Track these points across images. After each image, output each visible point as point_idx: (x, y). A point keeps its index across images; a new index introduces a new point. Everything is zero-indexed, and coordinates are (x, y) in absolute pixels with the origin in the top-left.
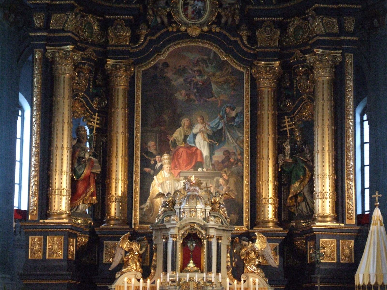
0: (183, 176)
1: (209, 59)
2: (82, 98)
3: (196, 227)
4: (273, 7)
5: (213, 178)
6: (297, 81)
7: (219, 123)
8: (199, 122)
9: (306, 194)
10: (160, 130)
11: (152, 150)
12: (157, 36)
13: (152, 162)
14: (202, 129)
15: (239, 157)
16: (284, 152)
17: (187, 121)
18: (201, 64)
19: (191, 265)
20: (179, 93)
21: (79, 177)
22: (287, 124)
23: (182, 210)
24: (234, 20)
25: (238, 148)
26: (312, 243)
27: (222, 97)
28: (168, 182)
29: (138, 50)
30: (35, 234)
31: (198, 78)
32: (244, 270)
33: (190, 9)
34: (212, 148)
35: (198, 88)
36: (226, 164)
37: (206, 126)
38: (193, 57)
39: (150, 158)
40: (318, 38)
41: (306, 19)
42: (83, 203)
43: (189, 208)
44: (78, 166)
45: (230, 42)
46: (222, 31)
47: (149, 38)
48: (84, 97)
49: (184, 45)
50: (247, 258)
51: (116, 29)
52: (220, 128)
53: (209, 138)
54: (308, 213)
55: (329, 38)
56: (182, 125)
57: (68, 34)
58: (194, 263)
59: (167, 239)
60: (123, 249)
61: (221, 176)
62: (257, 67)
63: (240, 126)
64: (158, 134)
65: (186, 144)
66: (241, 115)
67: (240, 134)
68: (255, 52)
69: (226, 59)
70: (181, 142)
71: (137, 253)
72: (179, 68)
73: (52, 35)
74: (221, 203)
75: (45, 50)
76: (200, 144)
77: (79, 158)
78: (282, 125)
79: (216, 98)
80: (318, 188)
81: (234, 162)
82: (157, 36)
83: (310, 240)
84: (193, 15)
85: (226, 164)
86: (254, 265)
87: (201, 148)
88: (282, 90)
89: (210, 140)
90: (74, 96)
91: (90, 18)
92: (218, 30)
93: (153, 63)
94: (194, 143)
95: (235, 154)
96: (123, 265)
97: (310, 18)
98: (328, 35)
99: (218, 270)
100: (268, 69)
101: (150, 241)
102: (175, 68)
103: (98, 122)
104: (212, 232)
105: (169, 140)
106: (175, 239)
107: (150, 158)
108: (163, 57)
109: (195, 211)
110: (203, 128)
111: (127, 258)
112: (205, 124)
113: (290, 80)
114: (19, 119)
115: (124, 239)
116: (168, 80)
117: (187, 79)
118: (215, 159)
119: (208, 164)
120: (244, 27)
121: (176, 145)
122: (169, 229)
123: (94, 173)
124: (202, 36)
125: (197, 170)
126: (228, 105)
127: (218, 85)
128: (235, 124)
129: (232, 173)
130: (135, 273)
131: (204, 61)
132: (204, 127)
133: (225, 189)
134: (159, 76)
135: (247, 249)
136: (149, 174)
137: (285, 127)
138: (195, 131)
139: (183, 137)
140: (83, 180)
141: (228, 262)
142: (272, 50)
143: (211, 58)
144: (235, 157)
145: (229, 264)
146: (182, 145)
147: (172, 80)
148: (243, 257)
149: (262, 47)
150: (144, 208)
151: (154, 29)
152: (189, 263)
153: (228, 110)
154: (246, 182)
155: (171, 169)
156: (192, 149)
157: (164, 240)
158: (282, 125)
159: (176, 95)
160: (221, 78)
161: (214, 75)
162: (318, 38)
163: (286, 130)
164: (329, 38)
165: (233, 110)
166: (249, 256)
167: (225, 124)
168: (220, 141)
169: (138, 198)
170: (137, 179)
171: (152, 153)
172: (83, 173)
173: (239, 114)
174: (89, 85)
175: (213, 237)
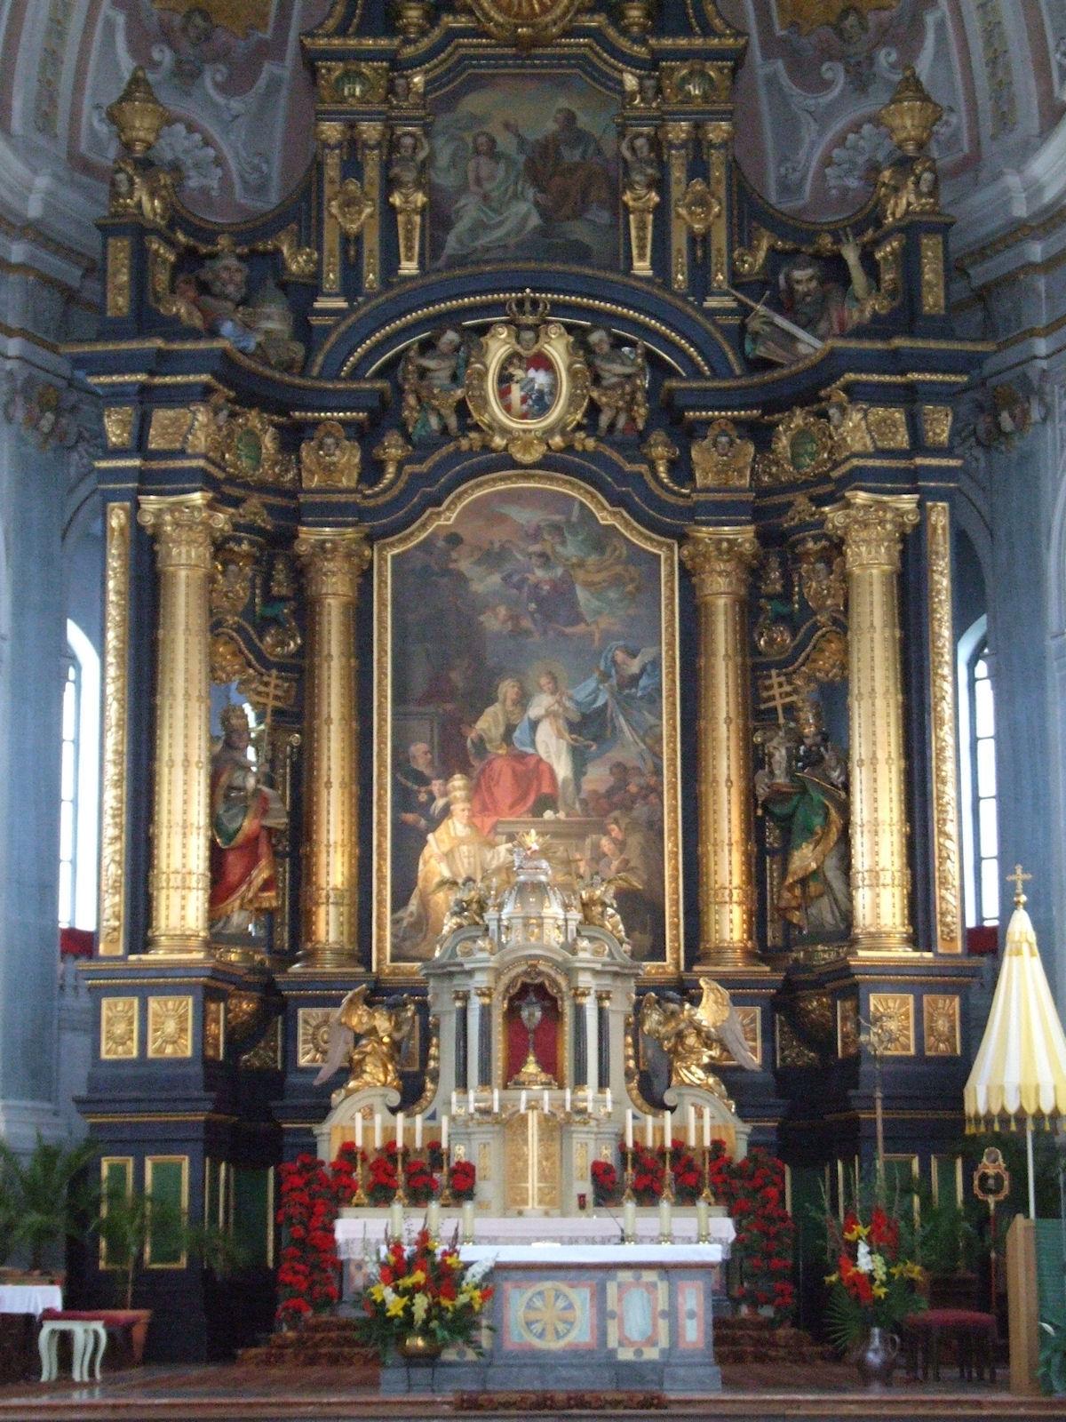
0: (503, 834)
1: (568, 521)
2: (237, 631)
3: (543, 967)
5: (582, 836)
6: (801, 577)
7: (596, 691)
10: (441, 711)
13: (423, 797)
15: (653, 780)
18: (546, 537)
19: (531, 1067)
20: (489, 613)
21: (230, 837)
22: (776, 691)
23: (505, 923)
25: (647, 756)
26: (848, 1005)
27: (604, 623)
28: (464, 848)
29: (381, 500)
30: (117, 992)
31: (540, 573)
32: (670, 1079)
33: (516, 393)
34: (580, 759)
35: (540, 601)
38: (524, 516)
40: (855, 462)
41: (823, 414)
42: (242, 907)
43: (523, 918)
45: (623, 477)
47: (408, 468)
48: (240, 629)
49: (501, 487)
50: (680, 1048)
51: (321, 447)
52: (599, 703)
53: (571, 732)
55: (886, 463)
56: (501, 697)
57: (195, 463)
58: (538, 1062)
59: (465, 997)
60: (349, 1029)
61: (607, 833)
62: (697, 541)
63: (653, 698)
67: (651, 720)
68: (689, 503)
69: (610, 521)
71: (386, 1040)
73: (154, 465)
74: (608, 901)
75: (137, 506)
77: (231, 788)
78: (765, 694)
79: (588, 625)
80: (861, 860)
81: (638, 793)
83: (845, 999)
84: (525, 407)
85: (615, 799)
86: (698, 1066)
88: (763, 600)
89: (574, 736)
90: (215, 627)
91: (254, 419)
92: (591, 443)
94: (533, 743)
95: (642, 775)
96: (349, 1070)
97: (833, 412)
99: (603, 1082)
101: (423, 1008)
103: (279, 693)
104: (585, 980)
106: (487, 1000)
107: (416, 787)
108: (447, 518)
109: (540, 926)
110: (556, 707)
111: (360, 1053)
112: (561, 695)
114: (70, 689)
115: (351, 1001)
116: (461, 578)
117: (510, 576)
119: (570, 801)
120: (658, 436)
123: (270, 830)
124: (548, 464)
126: (621, 643)
128: (639, 694)
131: (557, 529)
132: (559, 702)
133: (615, 864)
134: (436, 568)
135: (678, 1025)
137: (772, 698)
138: (534, 711)
139: (502, 730)
140: (240, 847)
141: (627, 1058)
142: (736, 497)
144: (642, 781)
145: (632, 1063)
146: (500, 752)
148: (667, 1045)
149: (707, 490)
152: (526, 1063)
153: (620, 656)
154: (672, 846)
155: (474, 816)
157: (459, 1004)
158: (765, 694)
159: (482, 618)
161: (581, 565)
162: (855, 462)
163: (775, 709)
164: (886, 463)
165: (635, 656)
166: (683, 1044)
167: (612, 694)
170: (383, 842)
172: (238, 830)
173: (649, 668)
174: (254, 594)
175: (589, 994)
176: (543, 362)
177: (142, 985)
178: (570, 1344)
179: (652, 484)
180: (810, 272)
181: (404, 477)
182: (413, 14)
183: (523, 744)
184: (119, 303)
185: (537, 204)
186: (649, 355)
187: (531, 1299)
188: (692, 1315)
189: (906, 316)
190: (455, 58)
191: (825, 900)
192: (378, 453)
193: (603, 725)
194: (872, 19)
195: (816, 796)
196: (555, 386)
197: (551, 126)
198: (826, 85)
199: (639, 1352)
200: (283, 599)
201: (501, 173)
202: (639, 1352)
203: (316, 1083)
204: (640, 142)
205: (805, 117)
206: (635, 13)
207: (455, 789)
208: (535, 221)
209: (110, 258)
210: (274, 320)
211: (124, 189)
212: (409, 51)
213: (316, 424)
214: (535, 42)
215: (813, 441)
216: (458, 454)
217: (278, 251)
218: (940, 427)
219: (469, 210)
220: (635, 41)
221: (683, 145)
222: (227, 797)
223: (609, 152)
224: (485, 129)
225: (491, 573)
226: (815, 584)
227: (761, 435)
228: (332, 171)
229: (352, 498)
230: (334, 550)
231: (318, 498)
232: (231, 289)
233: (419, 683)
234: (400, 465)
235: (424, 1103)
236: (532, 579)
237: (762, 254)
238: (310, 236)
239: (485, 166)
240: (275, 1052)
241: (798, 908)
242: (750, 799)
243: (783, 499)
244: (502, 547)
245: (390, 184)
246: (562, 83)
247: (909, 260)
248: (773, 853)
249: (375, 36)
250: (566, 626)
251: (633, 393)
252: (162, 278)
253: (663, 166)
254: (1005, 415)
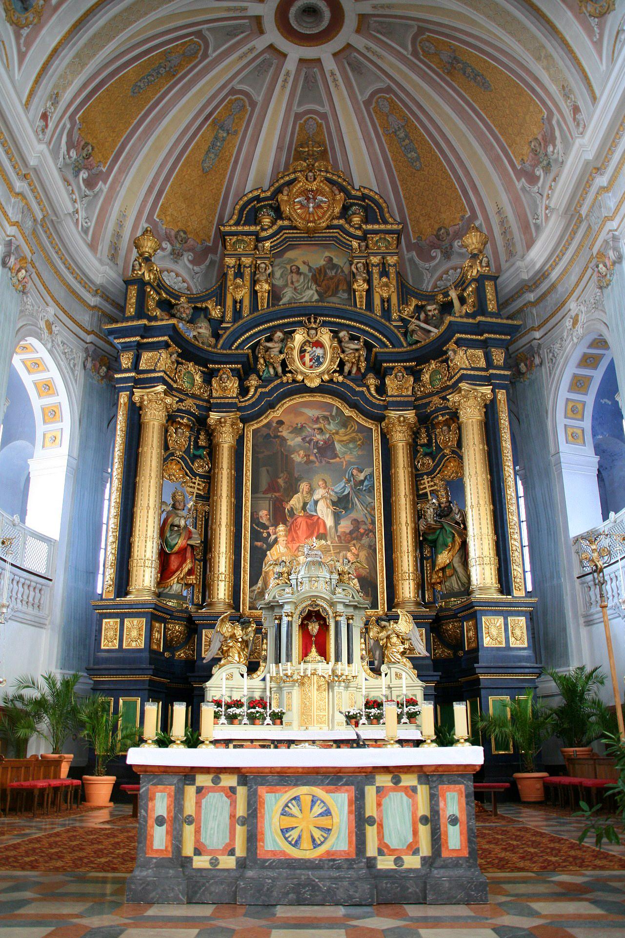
1: (331, 415)
3: (320, 602)
4: (405, 350)
7: (345, 486)
9: (456, 565)
11: (264, 520)
12: (269, 388)
13: (265, 535)
16: (425, 516)
19: (314, 652)
21: (172, 548)
22: (427, 485)
23: (300, 580)
24: (359, 369)
25: (368, 516)
27: (347, 458)
29: (247, 403)
30: (110, 616)
31: (318, 437)
33: (307, 358)
34: (337, 517)
35: (319, 448)
38: (312, 413)
40: (462, 372)
42: (178, 582)
44: (170, 536)
45: (355, 393)
46: (345, 381)
47: (260, 390)
48: (182, 458)
49: (301, 400)
51: (221, 380)
52: (346, 493)
54: (460, 589)
55: (476, 373)
56: (301, 490)
58: (317, 652)
59: (280, 619)
61: (350, 550)
63: (371, 490)
66: (370, 478)
67: (370, 500)
68: (385, 403)
71: (240, 640)
73: (142, 376)
75: (132, 393)
77: (172, 525)
78: (422, 487)
82: (269, 388)
83: (468, 620)
84: (311, 363)
85: (354, 535)
92: (341, 379)
93: (265, 421)
95: (365, 524)
98: (473, 369)
99: (350, 661)
100: (402, 419)
106: (290, 619)
108: (277, 414)
113: (427, 436)
114: (108, 485)
116: (284, 440)
117: (305, 438)
118: (341, 529)
119: (333, 536)
120: (371, 375)
122: (281, 606)
123: (192, 546)
124: (321, 389)
126: (356, 466)
129: (363, 546)
130: (238, 665)
131: (326, 418)
134: (272, 435)
136: (261, 548)
137: (425, 488)
139: (301, 504)
140: (177, 553)
141: (362, 650)
142: (406, 399)
143: (334, 414)
149: (392, 396)
150: (255, 590)
151: (266, 382)
153: (355, 472)
154: (381, 556)
157: (277, 622)
158: (422, 487)
159: (292, 456)
160: (345, 435)
161: (337, 433)
162: (462, 372)
164: (476, 373)
168: (346, 508)
169: (248, 577)
174: (190, 444)
176: (319, 344)
177: (121, 613)
178: (328, 852)
179: (368, 396)
180: (435, 306)
181: (258, 394)
182: (266, 221)
184: (131, 310)
185: (317, 291)
186: (366, 342)
187: (287, 805)
188: (454, 821)
189: (481, 308)
190: (283, 237)
191: (454, 578)
192: (247, 383)
193: (348, 502)
194: (451, 230)
195: (448, 528)
196: (325, 354)
197: (322, 262)
198: (434, 258)
199: (398, 861)
200: (204, 448)
201: (302, 280)
202: (398, 861)
203: (205, 661)
204: (359, 265)
205: (424, 271)
206: (356, 220)
208: (316, 297)
209: (129, 293)
210: (204, 329)
211: (137, 268)
212: (264, 234)
213: (218, 370)
214: (315, 230)
215: (440, 374)
216: (282, 384)
217: (207, 308)
218: (499, 356)
219: (288, 295)
220: (356, 229)
221: (378, 265)
222: (171, 530)
223: (346, 271)
224: (296, 263)
226: (444, 437)
227: (416, 374)
228: (231, 276)
229: (234, 401)
230: (225, 422)
231: (219, 401)
232: (184, 315)
233: (264, 484)
234: (256, 388)
235: (258, 673)
236: (315, 439)
237: (412, 308)
238: (221, 302)
239: (295, 276)
240: (193, 651)
241: (440, 583)
242: (416, 531)
243: (427, 400)
244: (302, 426)
245: (254, 282)
246: (326, 247)
247: (480, 293)
248: (427, 559)
249: (250, 225)
251: (359, 357)
252: (151, 304)
253: (369, 273)
254: (522, 364)
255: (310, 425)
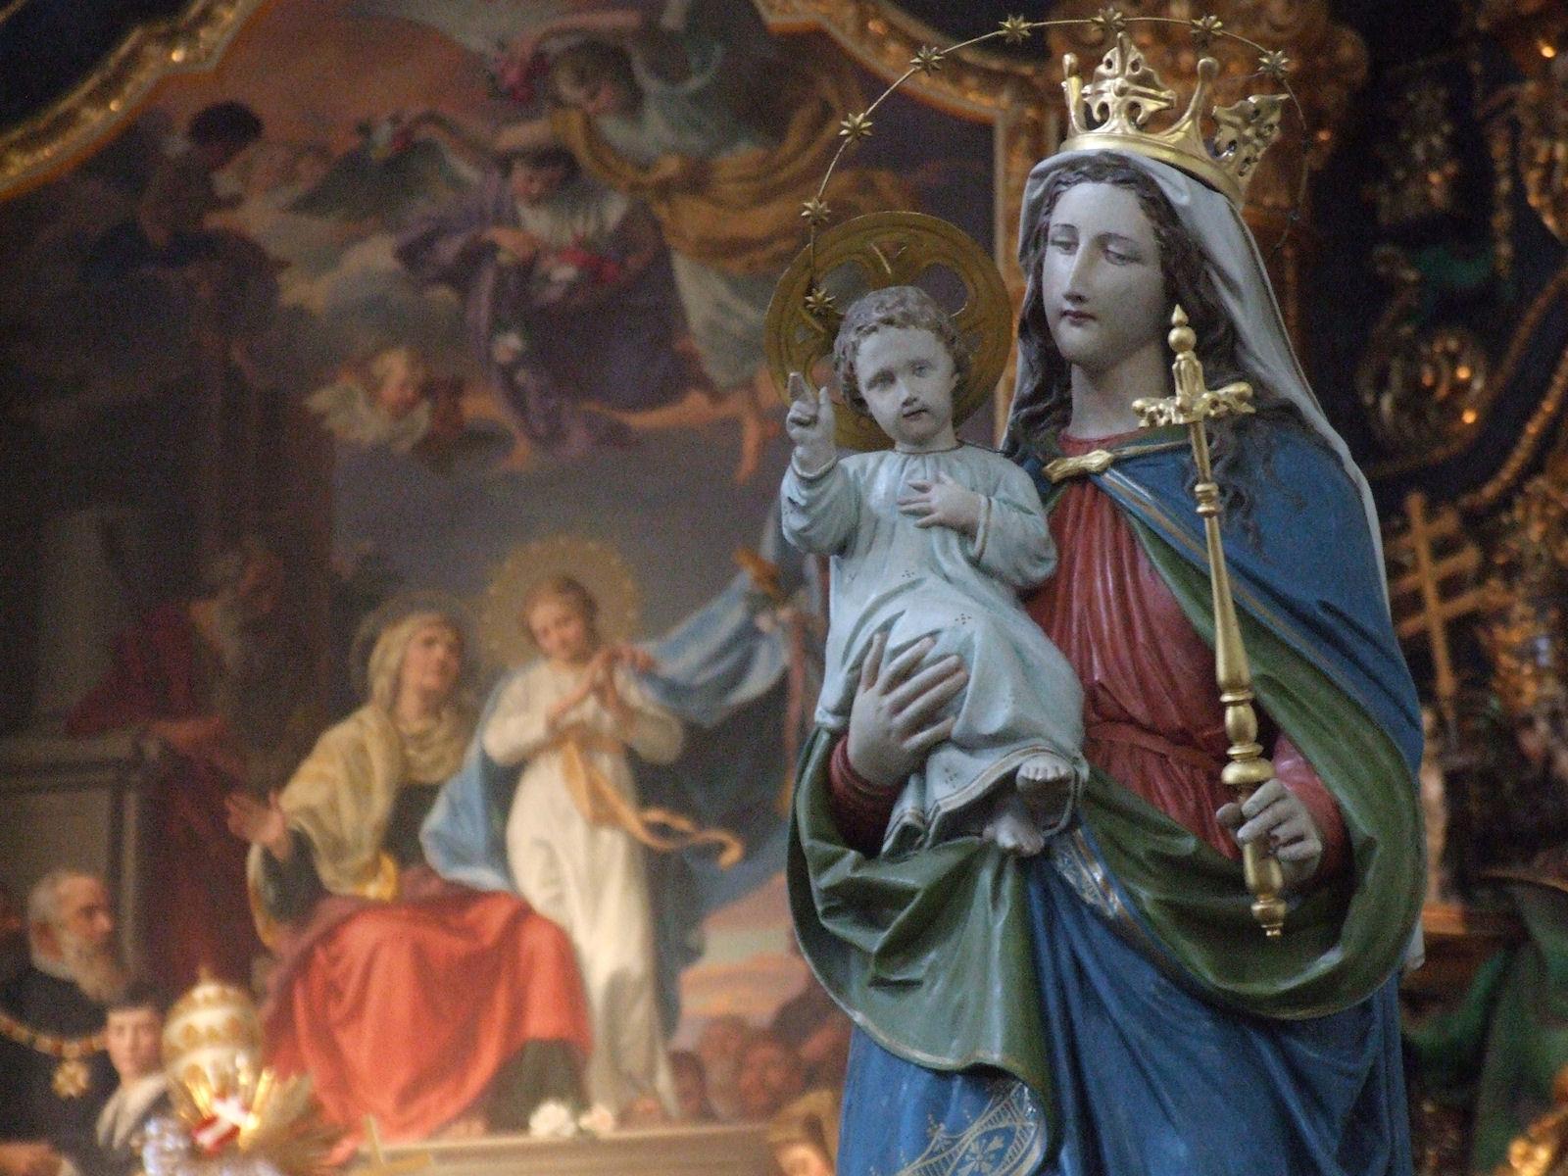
6: (1515, 126)
7: (748, 634)
8: (551, 642)
10: (152, 750)
13: (71, 1079)
14: (573, 716)
17: (429, 643)
18: (567, 89)
20: (347, 382)
31: (538, 223)
36: (816, 1045)
37: (621, 677)
39: (45, 1043)
52: (757, 683)
56: (381, 684)
64: (132, 800)
65: (415, 870)
70: (366, 856)
72: (354, 142)
76: (552, 862)
79: (716, 396)
87: (559, 899)
88: (1385, 250)
89: (656, 815)
94: (498, 852)
102: (321, 152)
105: (244, 847)
107: (45, 1043)
110: (591, 705)
112: (613, 659)
117: (428, 241)
119: (634, 1061)
121: (318, 891)
125: (521, 1125)
127: (737, 266)
134: (157, 235)
139: (380, 804)
146: (374, 890)
147: (283, 265)
156: (473, 914)
159: (321, 400)
160: (764, 198)
161: (696, 180)
171: (68, 987)
183: (459, 855)
207: (193, 1038)
225: (361, 238)
250: (634, 407)
255: (477, 127)
